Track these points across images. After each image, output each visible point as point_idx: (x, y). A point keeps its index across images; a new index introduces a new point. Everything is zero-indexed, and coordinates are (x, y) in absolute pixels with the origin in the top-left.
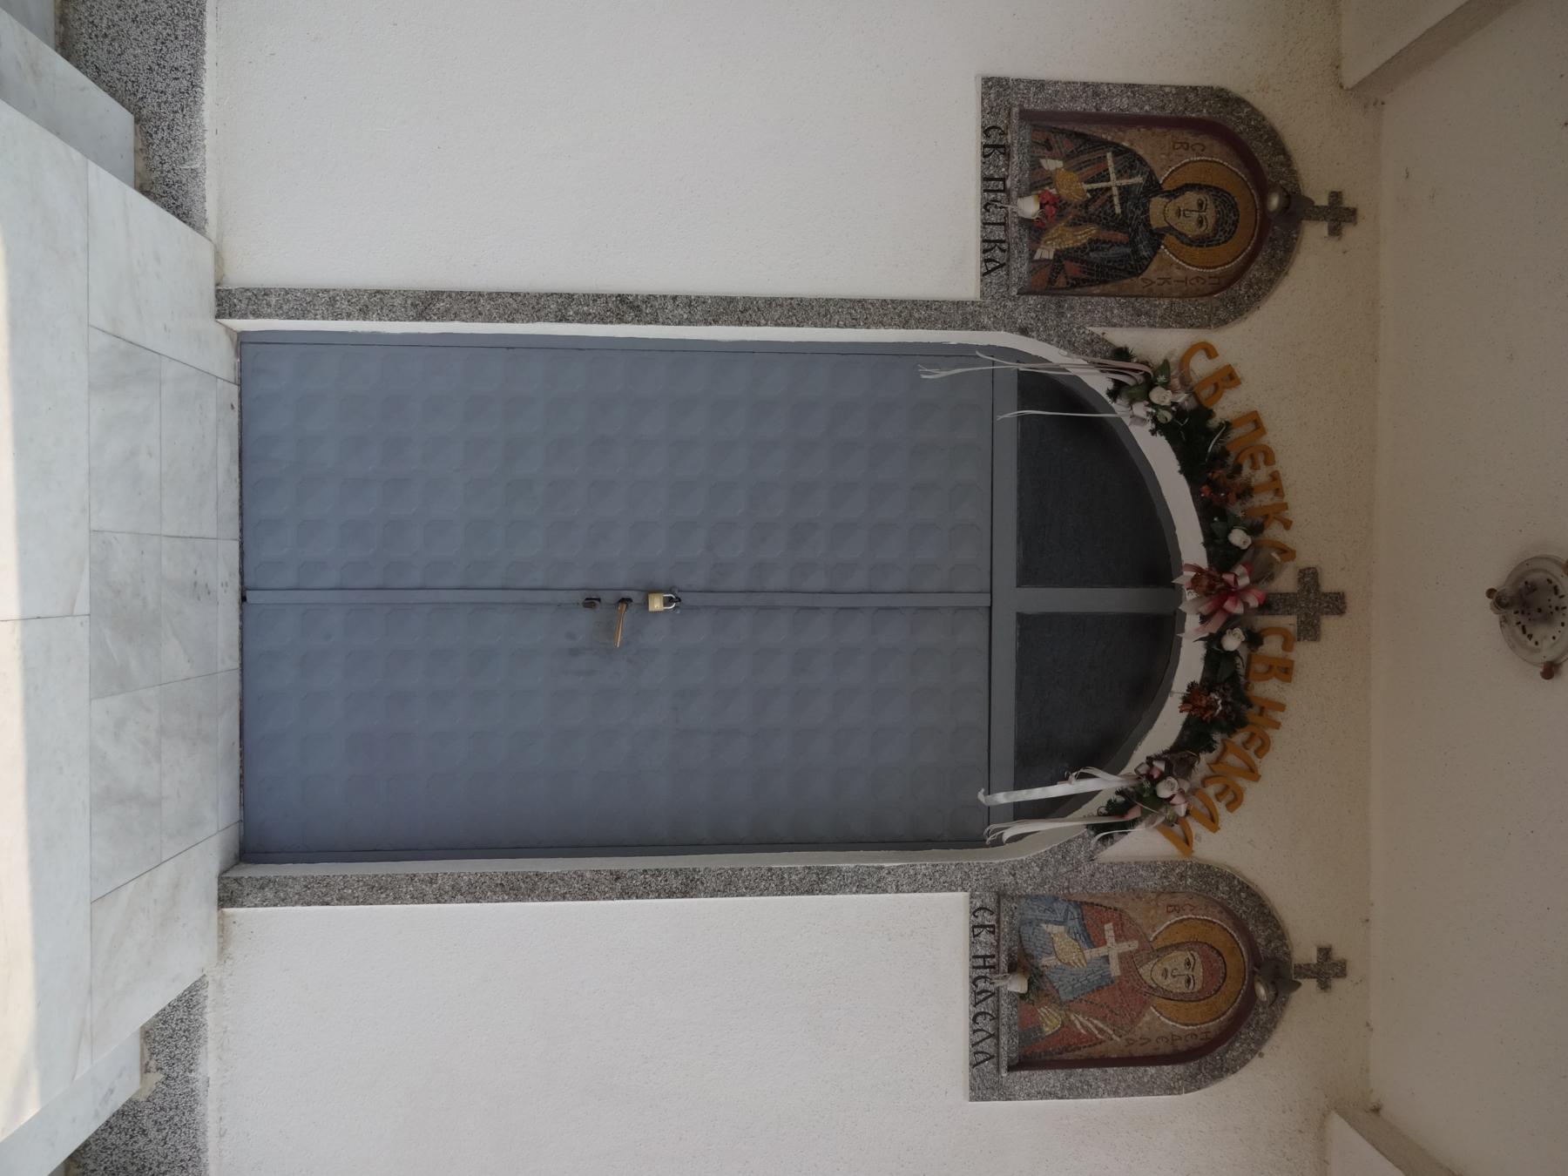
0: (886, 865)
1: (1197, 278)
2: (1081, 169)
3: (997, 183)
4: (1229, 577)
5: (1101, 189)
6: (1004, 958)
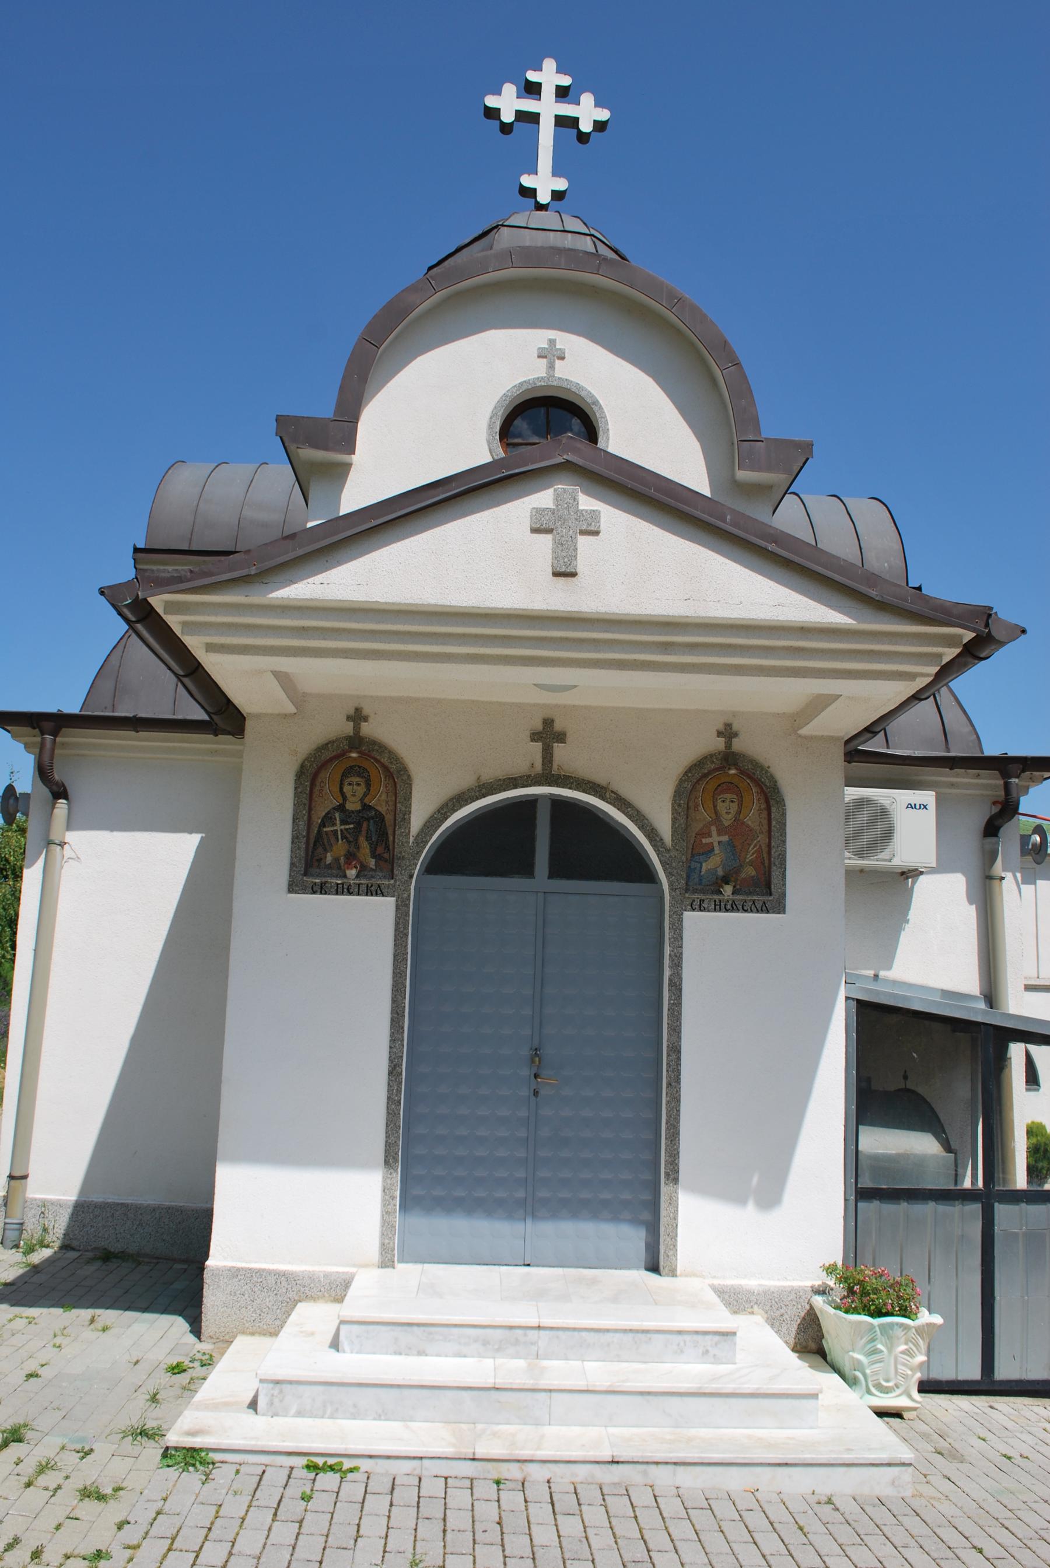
1: (386, 787)
5: (341, 834)
6: (716, 897)
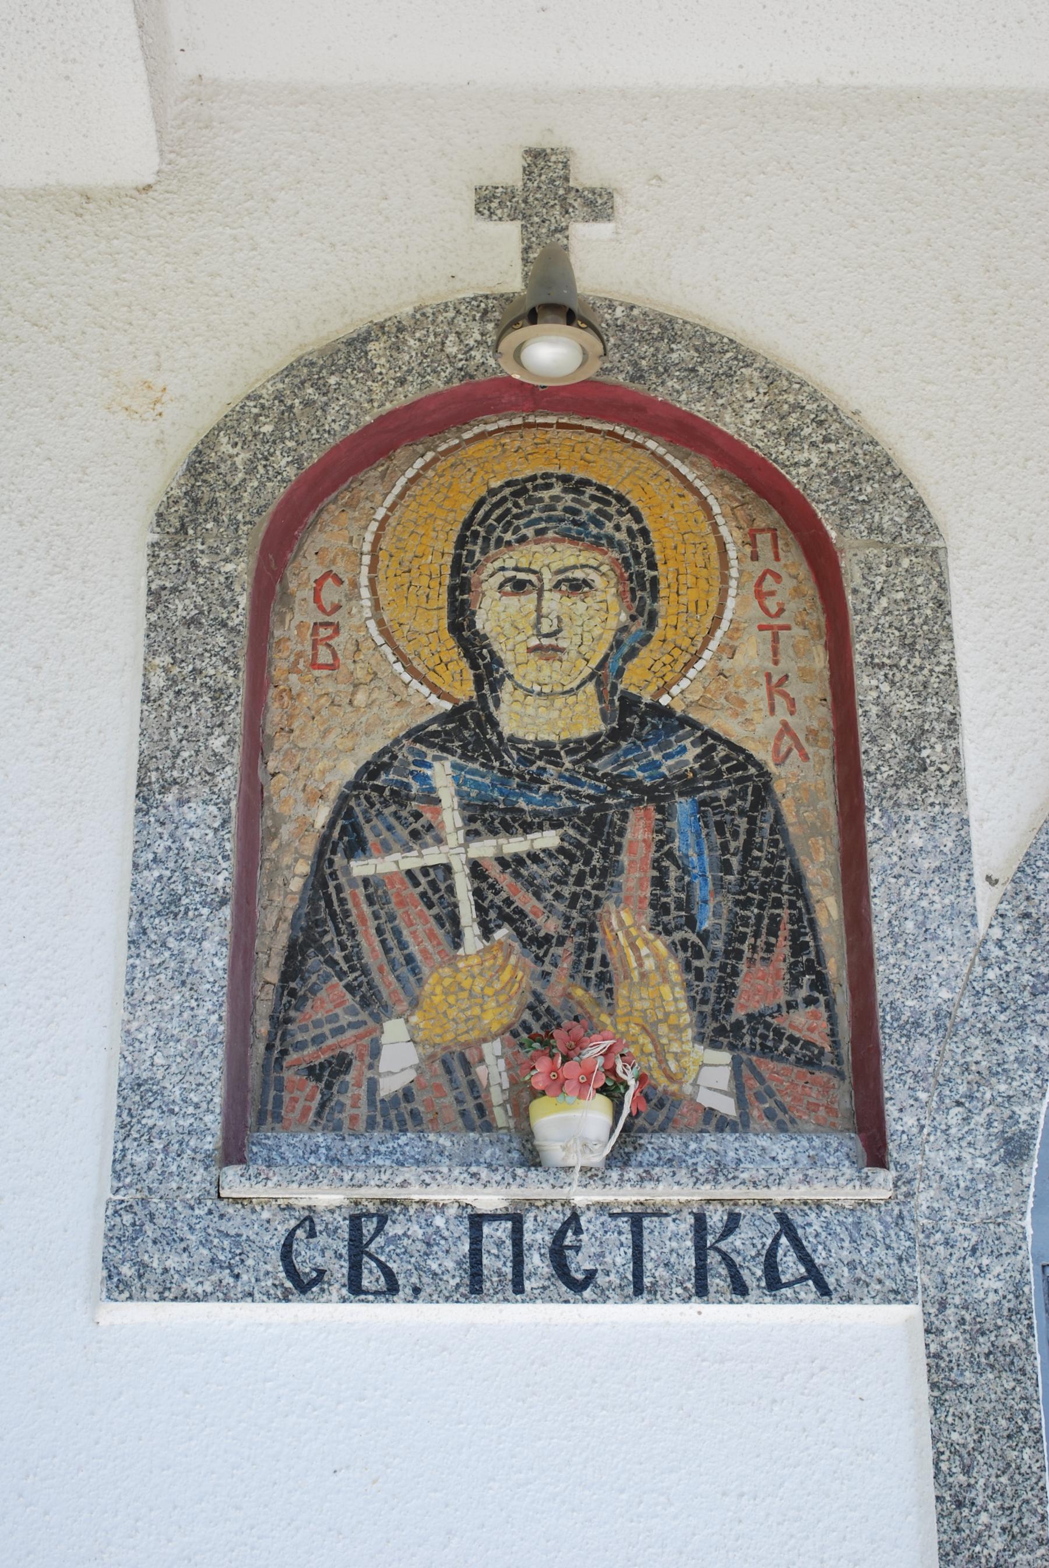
1: (760, 595)
2: (409, 959)
3: (487, 1244)
5: (477, 893)
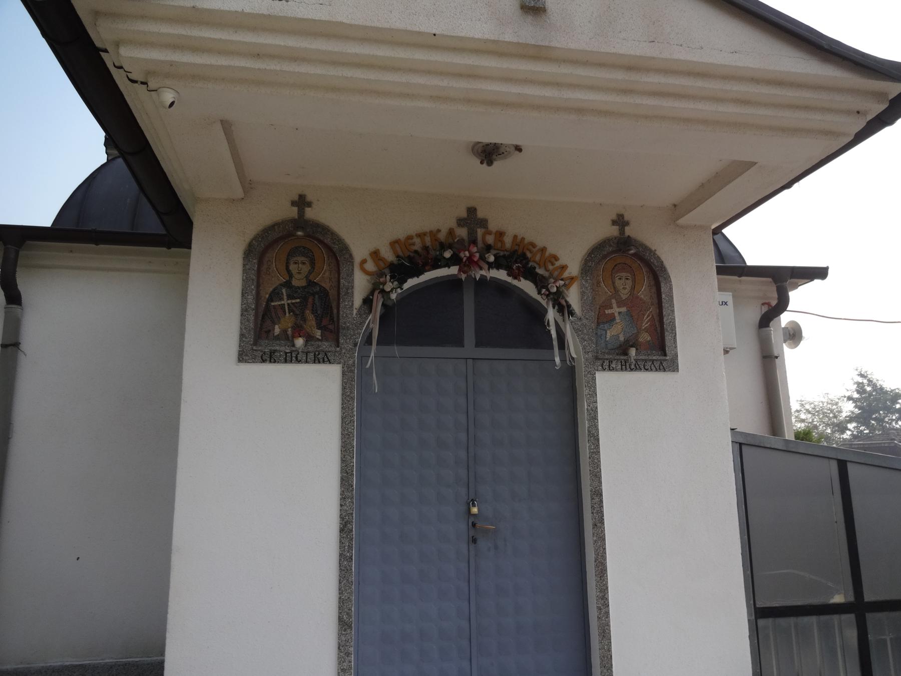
0: (586, 407)
1: (329, 266)
2: (279, 317)
4: (465, 259)
5: (288, 308)
6: (622, 357)
